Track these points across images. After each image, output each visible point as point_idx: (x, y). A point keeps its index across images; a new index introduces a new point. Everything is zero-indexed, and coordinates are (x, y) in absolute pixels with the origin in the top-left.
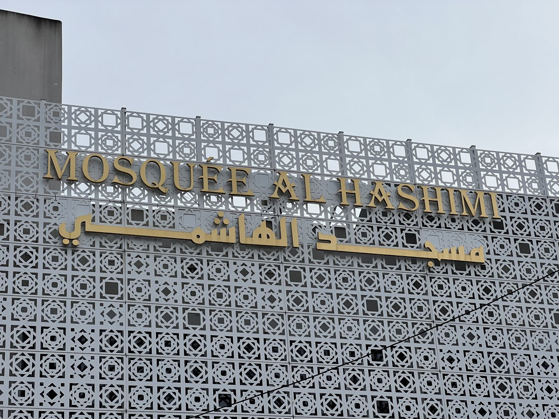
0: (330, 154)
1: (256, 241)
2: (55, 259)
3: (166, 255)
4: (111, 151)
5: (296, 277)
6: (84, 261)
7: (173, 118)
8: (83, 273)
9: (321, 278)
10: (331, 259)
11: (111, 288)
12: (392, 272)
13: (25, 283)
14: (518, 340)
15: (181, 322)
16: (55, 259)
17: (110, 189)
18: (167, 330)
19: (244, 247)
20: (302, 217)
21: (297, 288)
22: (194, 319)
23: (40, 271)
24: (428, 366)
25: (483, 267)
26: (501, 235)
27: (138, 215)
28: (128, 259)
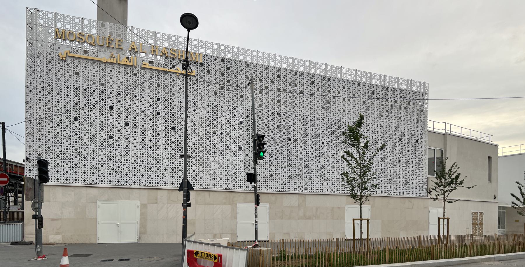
0: (93, 27)
1: (123, 63)
2: (59, 63)
3: (94, 65)
4: (77, 30)
5: (135, 75)
6: (68, 65)
7: (73, 17)
8: (68, 68)
9: (143, 76)
10: (147, 70)
11: (77, 74)
12: (166, 76)
13: (50, 70)
14: (202, 98)
15: (98, 85)
16: (59, 63)
17: (77, 43)
18: (94, 87)
19: (120, 64)
20: (139, 57)
21: (135, 78)
22: (103, 85)
23: (54, 66)
24: (173, 104)
25: (195, 77)
26: (202, 67)
27: (86, 52)
28: (82, 65)
